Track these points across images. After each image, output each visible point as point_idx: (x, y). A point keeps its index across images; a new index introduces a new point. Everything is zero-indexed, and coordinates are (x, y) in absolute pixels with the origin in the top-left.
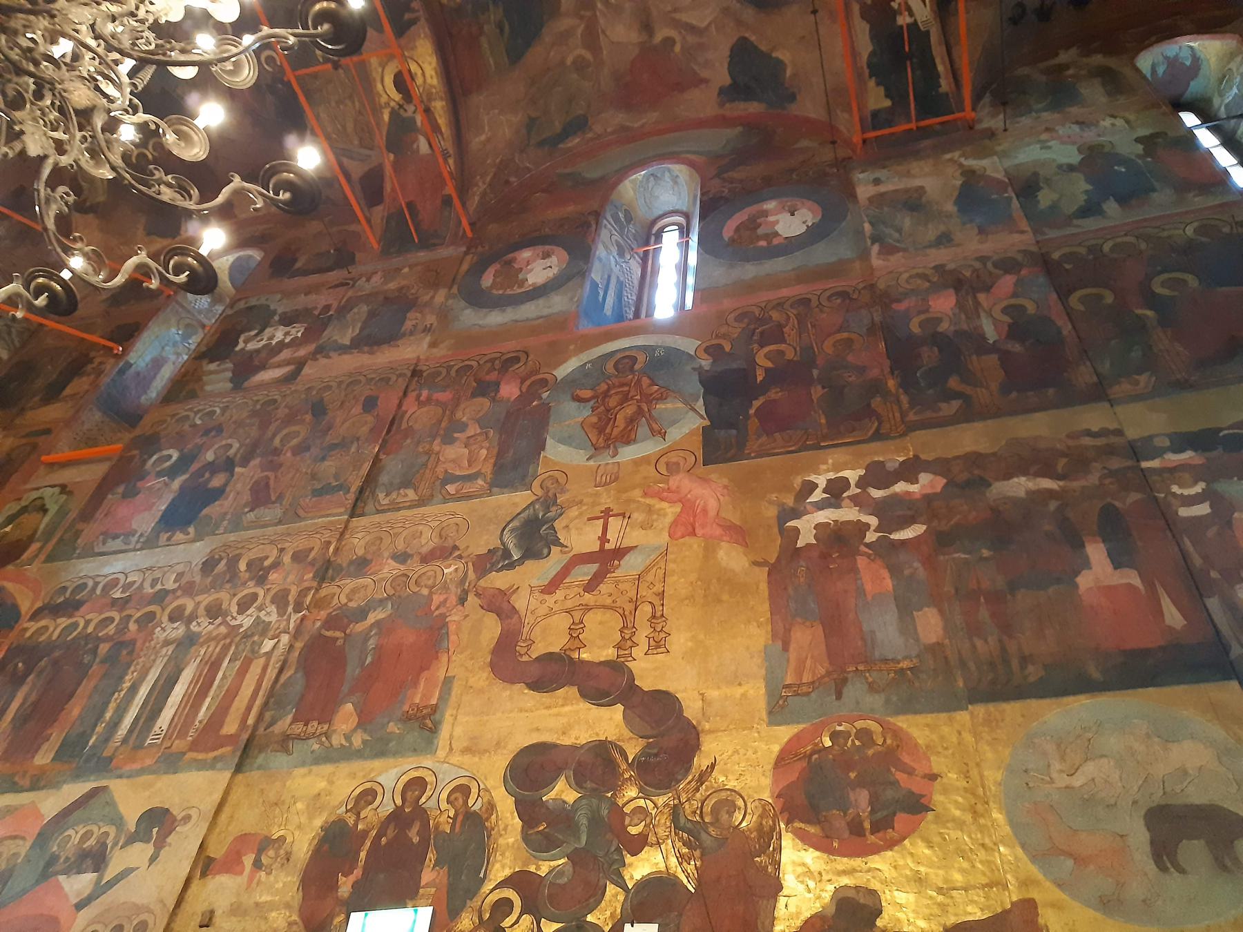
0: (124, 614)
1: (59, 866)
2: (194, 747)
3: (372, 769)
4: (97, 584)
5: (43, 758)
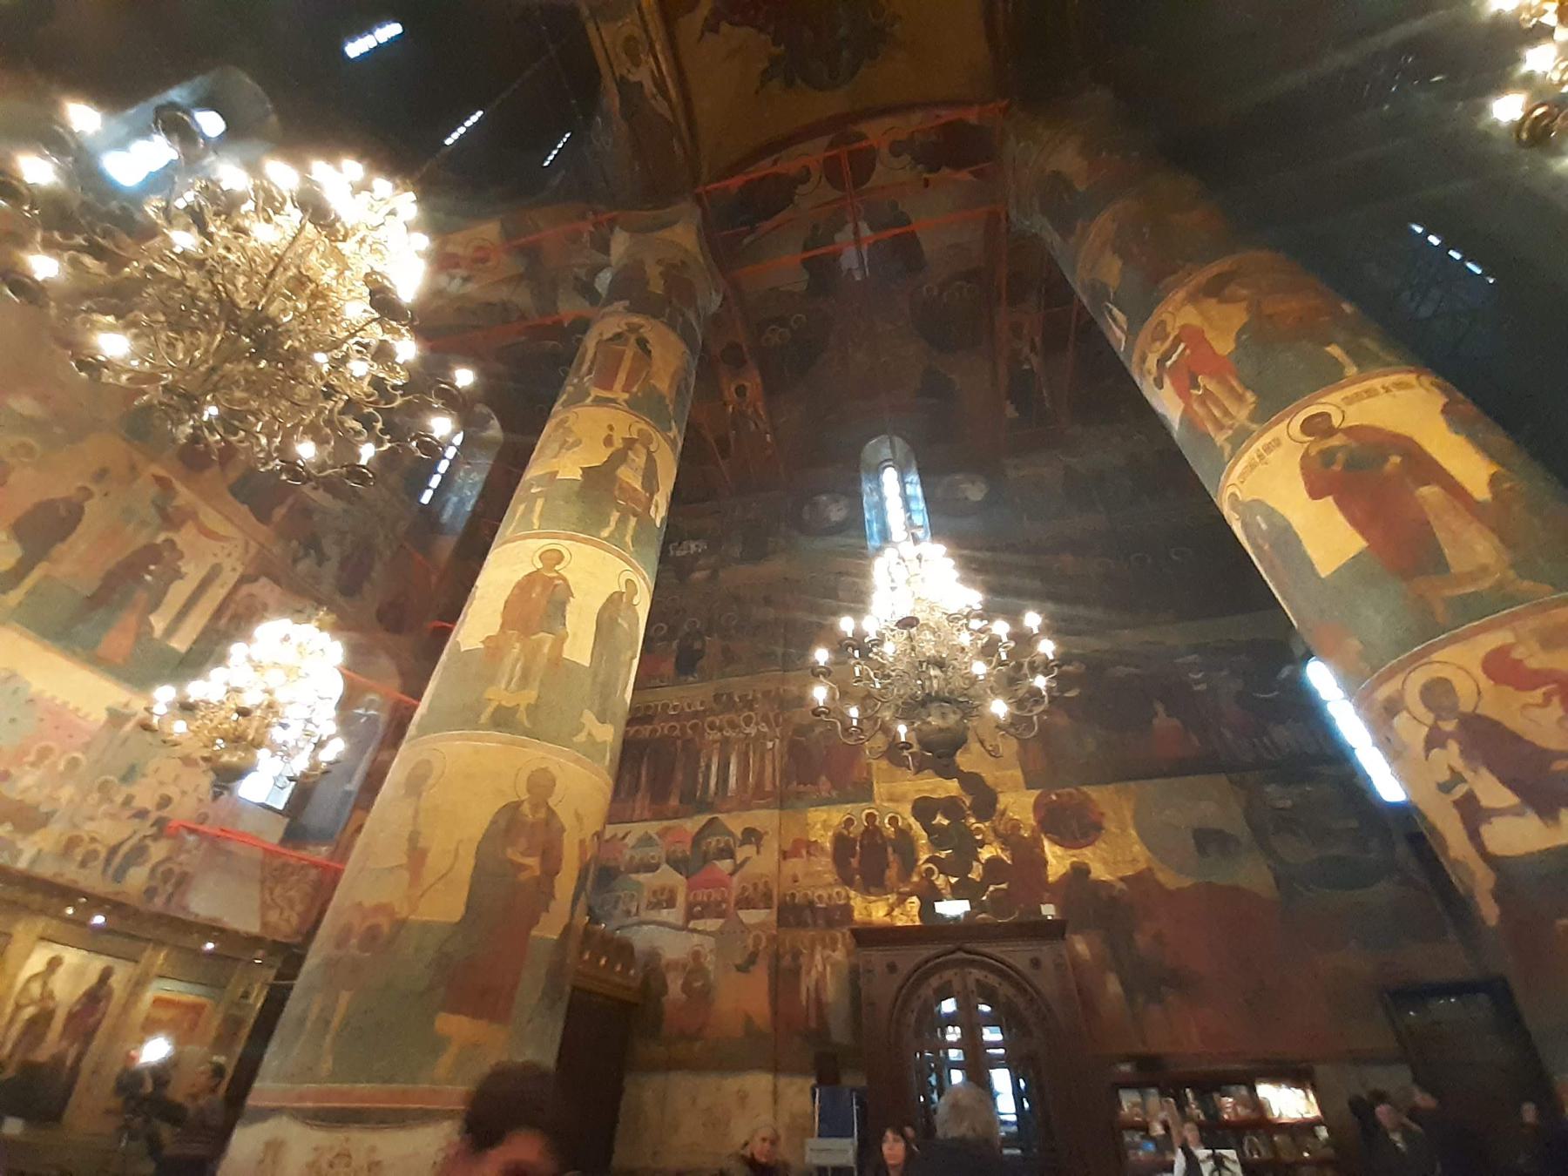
4: (657, 706)
5: (674, 802)
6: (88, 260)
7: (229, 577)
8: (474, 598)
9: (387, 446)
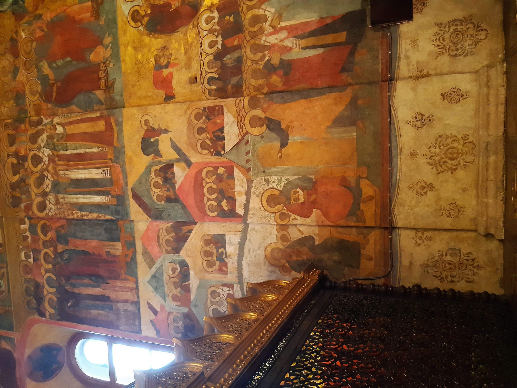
0: (41, 246)
1: (171, 194)
2: (110, 144)
3: (123, 21)
5: (118, 248)
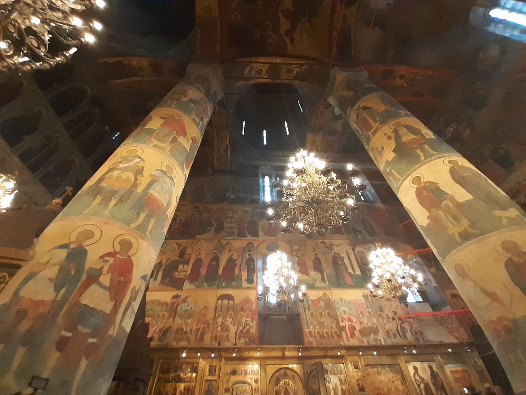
4: (514, 186)
6: (288, 217)
7: (350, 251)
8: (409, 211)
9: (354, 197)
